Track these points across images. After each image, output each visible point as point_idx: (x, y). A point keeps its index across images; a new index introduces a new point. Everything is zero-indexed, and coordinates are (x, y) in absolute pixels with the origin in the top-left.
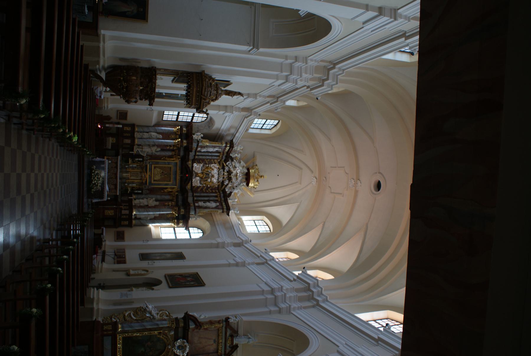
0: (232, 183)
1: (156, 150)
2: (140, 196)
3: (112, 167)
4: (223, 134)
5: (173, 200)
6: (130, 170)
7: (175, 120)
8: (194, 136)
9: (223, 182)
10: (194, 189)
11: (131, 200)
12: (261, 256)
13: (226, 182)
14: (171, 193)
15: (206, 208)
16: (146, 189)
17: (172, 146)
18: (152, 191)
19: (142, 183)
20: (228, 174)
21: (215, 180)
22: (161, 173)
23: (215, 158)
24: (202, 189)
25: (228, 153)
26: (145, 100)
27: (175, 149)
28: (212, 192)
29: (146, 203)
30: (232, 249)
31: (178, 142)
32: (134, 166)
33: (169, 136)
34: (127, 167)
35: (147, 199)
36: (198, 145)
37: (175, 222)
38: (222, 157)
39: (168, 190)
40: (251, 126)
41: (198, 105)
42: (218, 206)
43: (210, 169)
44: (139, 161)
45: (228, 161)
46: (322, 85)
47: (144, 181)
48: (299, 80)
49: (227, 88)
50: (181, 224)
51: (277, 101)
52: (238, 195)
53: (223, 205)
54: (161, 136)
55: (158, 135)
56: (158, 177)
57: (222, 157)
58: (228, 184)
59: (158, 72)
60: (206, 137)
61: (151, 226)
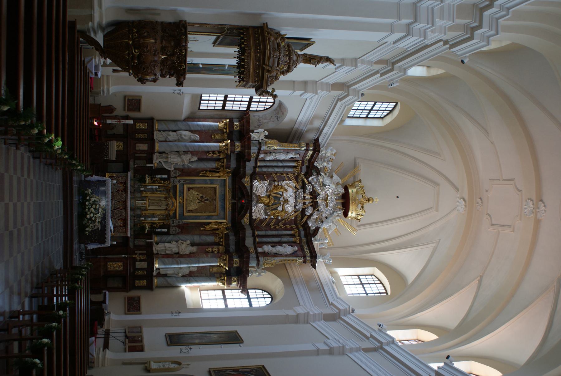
0: (318, 212)
1: (190, 159)
2: (165, 238)
3: (118, 190)
4: (302, 130)
5: (221, 243)
6: (148, 194)
7: (221, 108)
8: (253, 135)
9: (303, 211)
10: (255, 224)
11: (150, 245)
12: (372, 336)
13: (309, 211)
14: (217, 232)
15: (276, 255)
16: (174, 226)
17: (217, 153)
18: (185, 229)
19: (168, 217)
20: (312, 197)
21: (290, 208)
22: (199, 198)
23: (290, 170)
24: (268, 225)
26: (169, 77)
28: (286, 229)
29: (175, 250)
30: (321, 325)
31: (226, 145)
32: (154, 187)
33: (211, 135)
34: (142, 189)
35: (177, 242)
36: (259, 150)
37: (224, 279)
38: (301, 168)
39: (212, 227)
40: (349, 114)
41: (258, 82)
42: (297, 251)
43: (282, 190)
44: (161, 179)
46: (471, 38)
48: (429, 31)
49: (308, 51)
50: (234, 284)
51: (392, 70)
52: (329, 234)
53: (305, 249)
54: (197, 137)
56: (194, 206)
57: (301, 168)
58: (311, 215)
59: (189, 28)
60: (272, 135)
61: (185, 288)
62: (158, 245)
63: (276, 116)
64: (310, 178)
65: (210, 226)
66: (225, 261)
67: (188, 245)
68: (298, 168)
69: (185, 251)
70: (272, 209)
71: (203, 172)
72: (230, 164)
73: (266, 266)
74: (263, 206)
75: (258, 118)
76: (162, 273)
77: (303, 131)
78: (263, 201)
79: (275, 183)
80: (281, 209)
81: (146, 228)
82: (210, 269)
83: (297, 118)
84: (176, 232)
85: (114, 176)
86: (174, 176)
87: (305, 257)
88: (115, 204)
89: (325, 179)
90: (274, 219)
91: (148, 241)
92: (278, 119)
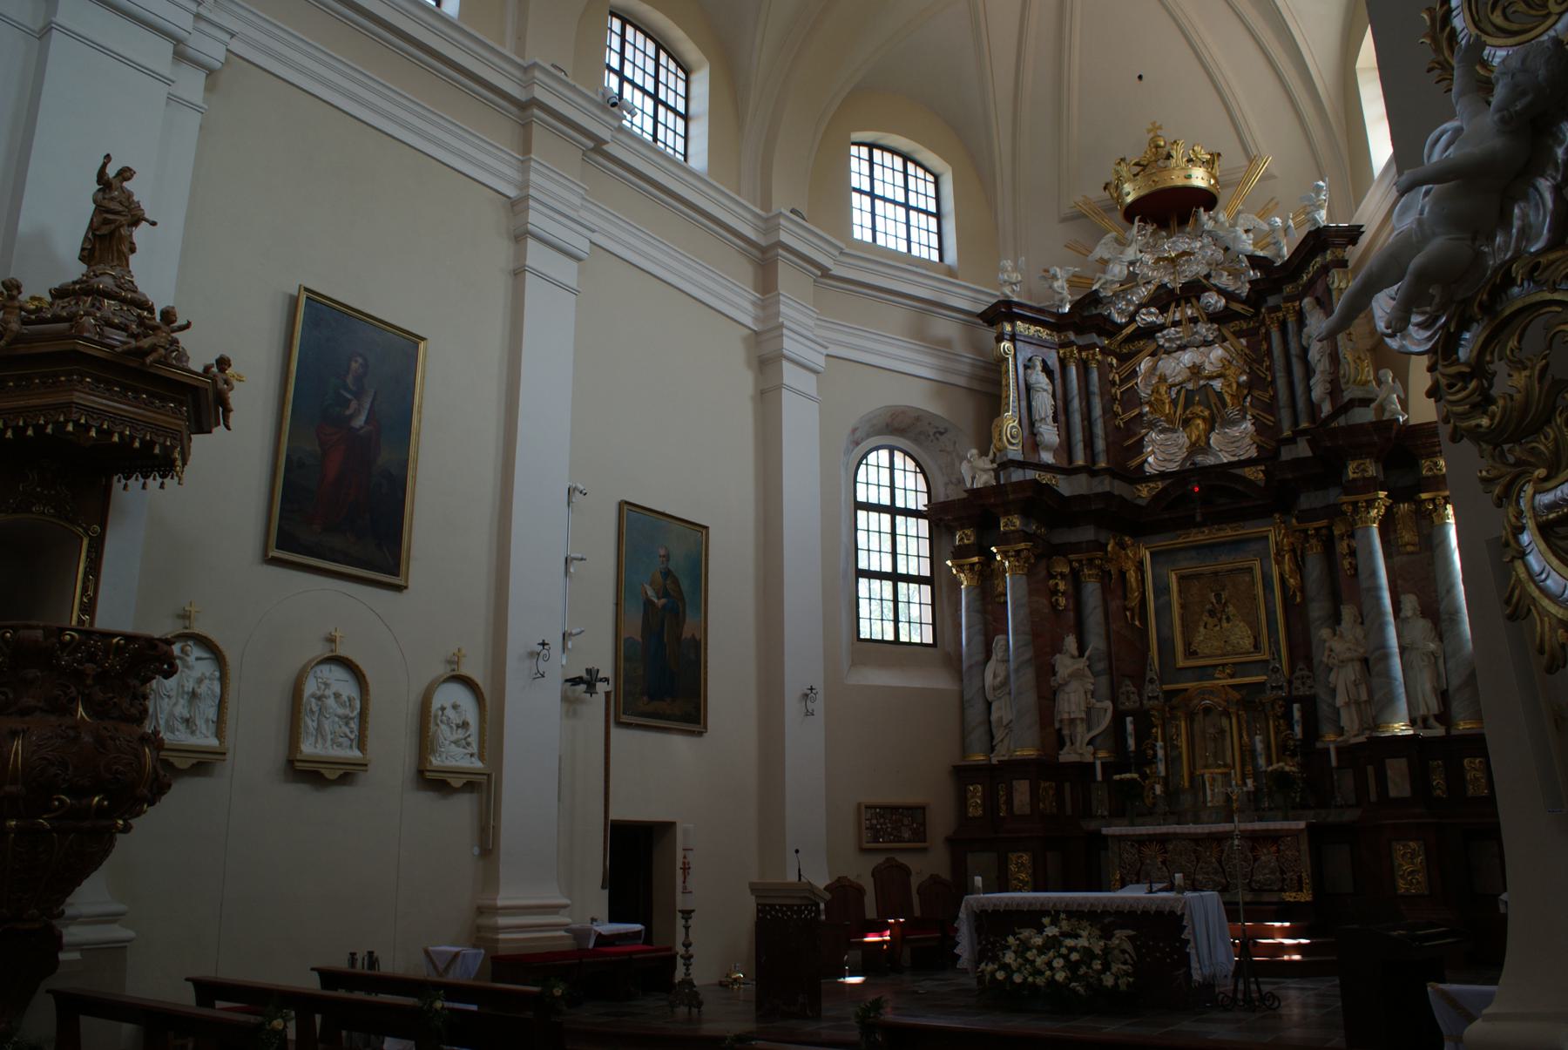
0: (1213, 274)
1: (1073, 657)
2: (1324, 710)
3: (1164, 862)
4: (973, 365)
5: (1324, 531)
9: (1215, 318)
11: (1345, 751)
13: (1214, 301)
15: (1335, 358)
17: (1052, 582)
18: (1301, 650)
20: (1173, 305)
23: (1095, 376)
25: (1059, 324)
27: (1066, 570)
28: (1269, 352)
35: (1331, 670)
37: (1433, 500)
39: (1291, 570)
40: (896, 251)
43: (1163, 389)
45: (1108, 319)
47: (1236, 695)
53: (1309, 276)
55: (994, 657)
56: (1241, 635)
58: (1221, 292)
63: (937, 439)
64: (1119, 321)
65: (1287, 576)
66: (1360, 504)
67: (1338, 632)
69: (1356, 639)
70: (1219, 405)
73: (1369, 375)
74: (1218, 434)
76: (1434, 706)
77: (982, 364)
78: (1199, 437)
80: (1222, 380)
81: (1283, 768)
83: (926, 381)
84: (1308, 677)
86: (1137, 698)
87: (1325, 270)
88: (1207, 873)
91: (1334, 763)
92: (942, 430)
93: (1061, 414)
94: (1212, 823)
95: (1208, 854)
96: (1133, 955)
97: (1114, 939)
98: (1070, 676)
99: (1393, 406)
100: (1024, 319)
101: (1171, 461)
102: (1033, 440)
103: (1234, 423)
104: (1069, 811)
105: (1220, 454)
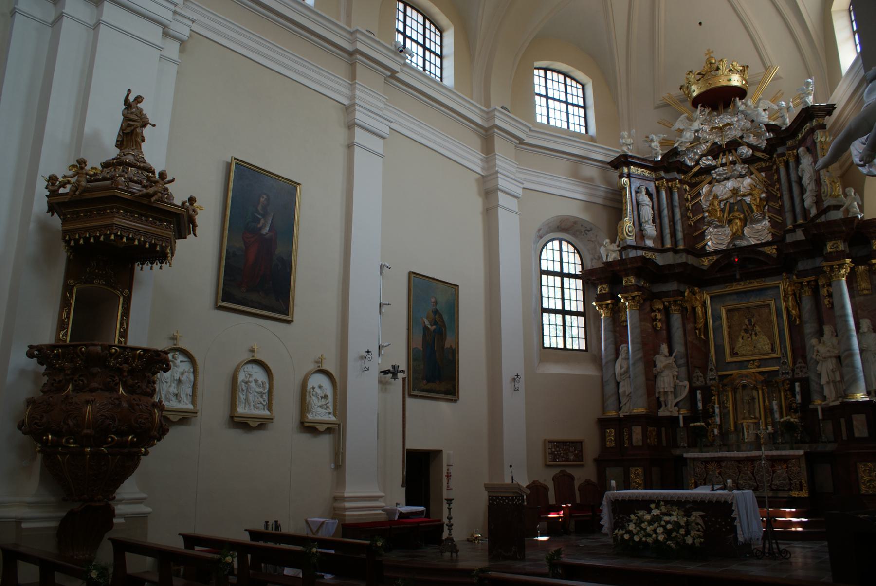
0: (745, 135)
1: (666, 356)
2: (814, 386)
3: (720, 474)
5: (813, 283)
9: (746, 161)
11: (827, 410)
13: (745, 151)
15: (818, 182)
17: (653, 314)
18: (800, 352)
20: (721, 154)
22: (749, 335)
25: (655, 167)
27: (661, 307)
28: (779, 178)
35: (818, 363)
39: (793, 305)
43: (716, 203)
45: (683, 164)
55: (620, 357)
56: (763, 344)
58: (750, 146)
62: (827, 397)
63: (587, 234)
64: (690, 165)
65: (791, 309)
66: (834, 267)
67: (822, 341)
68: (672, 184)
70: (749, 211)
71: (698, 334)
72: (673, 291)
73: (839, 191)
75: (594, 261)
77: (611, 191)
78: (737, 230)
79: (707, 216)
80: (751, 197)
81: (790, 420)
82: (865, 295)
83: (579, 201)
84: (804, 367)
85: (695, 481)
86: (703, 380)
87: (812, 131)
88: (745, 480)
89: (685, 140)
90: (769, 206)
91: (820, 416)
92: (589, 229)
93: (657, 218)
94: (748, 451)
95: (746, 468)
96: (704, 526)
97: (692, 517)
98: (665, 367)
99: (855, 209)
100: (635, 165)
101: (721, 244)
102: (641, 234)
103: (758, 221)
104: (664, 444)
105: (750, 239)
